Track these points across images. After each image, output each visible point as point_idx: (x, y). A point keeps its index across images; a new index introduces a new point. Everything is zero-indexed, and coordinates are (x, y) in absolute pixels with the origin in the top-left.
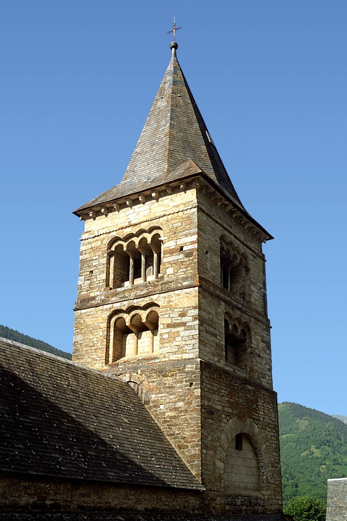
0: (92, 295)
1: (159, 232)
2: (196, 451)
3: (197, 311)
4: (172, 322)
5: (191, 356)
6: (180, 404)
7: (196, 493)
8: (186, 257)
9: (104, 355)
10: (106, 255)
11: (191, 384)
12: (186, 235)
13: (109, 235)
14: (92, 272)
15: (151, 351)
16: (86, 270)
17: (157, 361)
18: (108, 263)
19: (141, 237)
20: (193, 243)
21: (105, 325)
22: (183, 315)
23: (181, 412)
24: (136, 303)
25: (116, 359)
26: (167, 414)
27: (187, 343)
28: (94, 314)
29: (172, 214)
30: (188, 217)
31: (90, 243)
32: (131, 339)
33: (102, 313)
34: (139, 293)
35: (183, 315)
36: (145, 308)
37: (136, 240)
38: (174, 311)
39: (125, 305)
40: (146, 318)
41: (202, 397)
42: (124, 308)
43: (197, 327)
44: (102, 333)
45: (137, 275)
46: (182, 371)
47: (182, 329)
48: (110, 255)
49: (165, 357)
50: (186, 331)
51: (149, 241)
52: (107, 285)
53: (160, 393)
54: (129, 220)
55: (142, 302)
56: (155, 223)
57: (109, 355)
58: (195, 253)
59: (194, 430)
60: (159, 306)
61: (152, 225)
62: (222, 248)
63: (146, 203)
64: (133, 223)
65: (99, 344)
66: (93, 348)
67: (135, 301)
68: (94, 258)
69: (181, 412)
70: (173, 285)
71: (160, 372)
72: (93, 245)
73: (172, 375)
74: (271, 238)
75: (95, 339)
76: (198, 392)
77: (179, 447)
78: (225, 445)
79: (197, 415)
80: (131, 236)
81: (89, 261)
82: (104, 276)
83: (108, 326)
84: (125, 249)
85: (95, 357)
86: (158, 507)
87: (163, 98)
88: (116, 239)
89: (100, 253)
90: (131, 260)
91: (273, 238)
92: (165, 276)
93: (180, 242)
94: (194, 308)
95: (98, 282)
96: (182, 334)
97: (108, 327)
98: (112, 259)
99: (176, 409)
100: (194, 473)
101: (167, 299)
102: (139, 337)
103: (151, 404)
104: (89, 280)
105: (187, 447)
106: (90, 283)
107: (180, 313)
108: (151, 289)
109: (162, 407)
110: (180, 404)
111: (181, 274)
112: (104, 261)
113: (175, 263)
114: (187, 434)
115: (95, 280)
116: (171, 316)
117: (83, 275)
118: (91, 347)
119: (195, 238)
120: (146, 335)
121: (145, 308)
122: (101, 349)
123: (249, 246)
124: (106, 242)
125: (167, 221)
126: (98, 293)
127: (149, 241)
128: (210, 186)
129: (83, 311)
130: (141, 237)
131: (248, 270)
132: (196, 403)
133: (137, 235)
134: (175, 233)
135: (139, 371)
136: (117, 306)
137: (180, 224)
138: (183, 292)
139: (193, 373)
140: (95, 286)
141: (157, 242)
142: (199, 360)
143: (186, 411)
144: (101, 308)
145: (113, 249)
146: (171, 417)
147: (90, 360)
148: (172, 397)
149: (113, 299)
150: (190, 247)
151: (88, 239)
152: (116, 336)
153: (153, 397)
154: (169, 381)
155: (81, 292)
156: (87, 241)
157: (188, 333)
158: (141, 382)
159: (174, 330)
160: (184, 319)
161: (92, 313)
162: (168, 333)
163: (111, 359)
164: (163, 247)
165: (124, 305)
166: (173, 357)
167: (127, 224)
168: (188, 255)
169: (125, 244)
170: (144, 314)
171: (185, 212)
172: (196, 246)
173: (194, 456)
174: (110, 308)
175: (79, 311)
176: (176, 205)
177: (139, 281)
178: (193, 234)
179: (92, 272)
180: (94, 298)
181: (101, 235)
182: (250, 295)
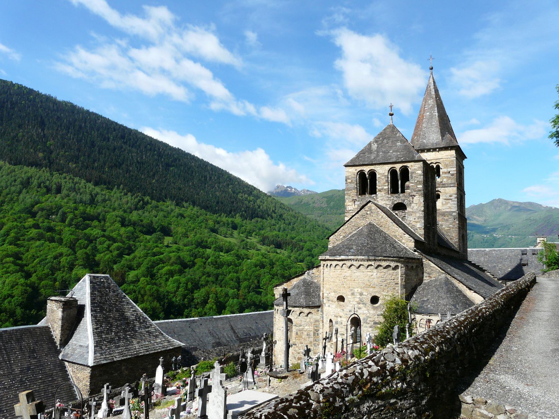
1: (439, 164)
3: (456, 196)
5: (454, 210)
12: (451, 168)
20: (454, 171)
22: (451, 196)
35: (451, 196)
46: (451, 215)
47: (450, 201)
51: (435, 167)
56: (438, 161)
58: (455, 175)
70: (446, 185)
76: (457, 222)
77: (451, 239)
93: (449, 170)
96: (450, 203)
99: (449, 227)
100: (456, 247)
111: (450, 181)
113: (447, 177)
119: (455, 169)
127: (435, 167)
132: (457, 226)
134: (446, 166)
150: (453, 172)
153: (440, 223)
154: (446, 218)
157: (453, 202)
159: (447, 201)
160: (451, 198)
166: (448, 210)
168: (452, 175)
172: (456, 172)
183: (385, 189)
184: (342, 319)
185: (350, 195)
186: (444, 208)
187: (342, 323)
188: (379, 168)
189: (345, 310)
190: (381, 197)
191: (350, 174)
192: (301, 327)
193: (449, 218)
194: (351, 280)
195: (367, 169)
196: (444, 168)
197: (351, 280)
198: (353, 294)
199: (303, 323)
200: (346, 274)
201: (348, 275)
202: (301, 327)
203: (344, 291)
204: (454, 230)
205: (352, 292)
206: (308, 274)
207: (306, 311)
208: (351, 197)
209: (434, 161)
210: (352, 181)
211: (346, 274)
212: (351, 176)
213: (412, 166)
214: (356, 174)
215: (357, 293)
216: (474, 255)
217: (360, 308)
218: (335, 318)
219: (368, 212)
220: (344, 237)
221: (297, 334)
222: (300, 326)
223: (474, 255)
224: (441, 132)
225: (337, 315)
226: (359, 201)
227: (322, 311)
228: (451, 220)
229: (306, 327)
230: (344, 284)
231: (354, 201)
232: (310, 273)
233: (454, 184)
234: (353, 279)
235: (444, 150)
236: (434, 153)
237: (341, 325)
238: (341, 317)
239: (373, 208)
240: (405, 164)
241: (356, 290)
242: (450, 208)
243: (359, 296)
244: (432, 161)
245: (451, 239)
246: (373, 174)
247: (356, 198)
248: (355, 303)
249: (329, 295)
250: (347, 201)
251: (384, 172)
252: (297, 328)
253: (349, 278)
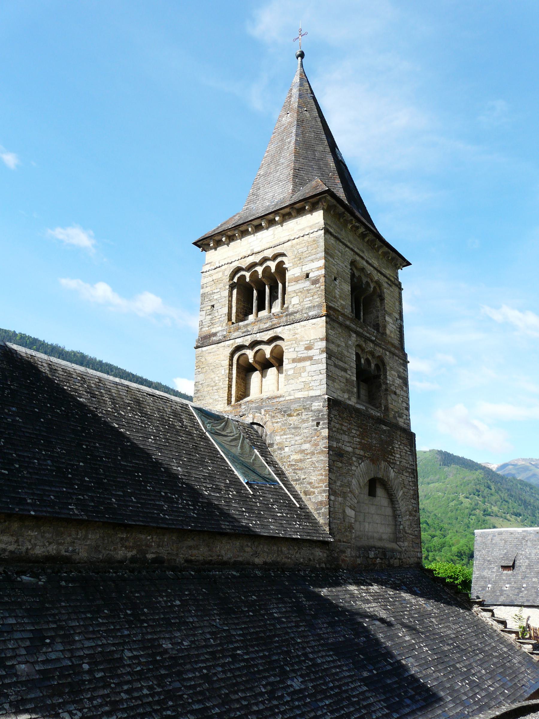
0: (214, 331)
2: (323, 497)
3: (323, 344)
4: (297, 356)
5: (318, 393)
6: (306, 446)
7: (325, 543)
8: (312, 284)
9: (226, 395)
10: (228, 287)
11: (318, 424)
12: (312, 261)
13: (231, 265)
14: (213, 306)
15: (275, 389)
16: (208, 304)
17: (281, 399)
18: (231, 295)
19: (264, 266)
20: (319, 269)
21: (227, 362)
22: (309, 348)
23: (307, 454)
25: (239, 399)
26: (292, 457)
27: (314, 378)
28: (216, 351)
29: (297, 238)
30: (314, 241)
31: (211, 275)
32: (256, 377)
33: (225, 349)
34: (263, 326)
35: (309, 348)
36: (270, 342)
37: (260, 270)
38: (299, 344)
39: (247, 341)
40: (270, 353)
41: (330, 438)
42: (247, 344)
43: (324, 361)
44: (224, 371)
45: (261, 307)
47: (308, 363)
48: (232, 287)
49: (290, 395)
50: (312, 366)
51: (273, 270)
52: (230, 319)
53: (284, 434)
54: (251, 248)
55: (266, 336)
56: (278, 250)
57: (231, 395)
58: (322, 280)
59: (322, 475)
60: (283, 339)
61: (276, 252)
62: (353, 275)
63: (269, 229)
64: (256, 250)
65: (221, 383)
66: (215, 388)
68: (216, 291)
69: (307, 454)
70: (298, 316)
71: (285, 412)
72: (215, 277)
73: (298, 414)
74: (411, 264)
75: (217, 378)
76: (325, 432)
77: (306, 493)
78: (356, 490)
79: (324, 458)
80: (254, 265)
81: (211, 294)
82: (226, 310)
83: (230, 364)
84: (248, 280)
85: (217, 397)
86: (278, 560)
87: (288, 113)
88: (239, 269)
89: (222, 285)
90: (255, 292)
91: (411, 264)
92: (290, 307)
93: (306, 269)
94: (322, 340)
95: (220, 316)
96: (308, 369)
97: (231, 365)
98: (235, 292)
99: (302, 451)
101: (292, 332)
102: (263, 375)
103: (275, 447)
104: (210, 314)
105: (314, 493)
106: (211, 318)
107: (306, 346)
108: (275, 321)
109: (287, 449)
110: (306, 446)
111: (307, 303)
112: (226, 293)
114: (314, 478)
116: (296, 350)
117: (204, 309)
119: (322, 262)
120: (272, 372)
121: (270, 342)
122: (222, 388)
123: (384, 272)
124: (228, 273)
125: (292, 246)
126: (220, 328)
127: (273, 270)
128: (338, 205)
129: (204, 349)
130: (264, 266)
131: (382, 299)
132: (323, 444)
133: (261, 263)
134: (300, 259)
135: (263, 411)
136: (239, 342)
137: (305, 249)
138: (310, 323)
139: (320, 411)
141: (281, 270)
142: (326, 397)
143: (313, 454)
144: (222, 344)
145: (235, 280)
146: (297, 461)
147: (211, 401)
148: (297, 438)
151: (209, 271)
152: (239, 375)
153: (278, 439)
154: (293, 420)
156: (208, 273)
157: (314, 368)
158: (265, 423)
159: (300, 365)
160: (310, 353)
161: (213, 350)
162: (294, 368)
163: (233, 399)
164: (288, 275)
166: (299, 395)
167: (249, 253)
168: (315, 282)
169: (248, 275)
170: (267, 350)
171: (311, 235)
172: (323, 272)
173: (321, 503)
174: (232, 344)
175: (200, 349)
176: (301, 228)
177: (263, 314)
178: (320, 259)
179: (213, 306)
180: (215, 334)
181: (222, 265)
182: (385, 327)
186: (290, 388)
193: (304, 421)
196: (295, 265)
204: (314, 459)
209: (269, 254)
216: (529, 544)
223: (529, 544)
224: (295, 176)
228: (307, 428)
233: (319, 306)
235: (295, 217)
242: (307, 386)
245: (306, 493)
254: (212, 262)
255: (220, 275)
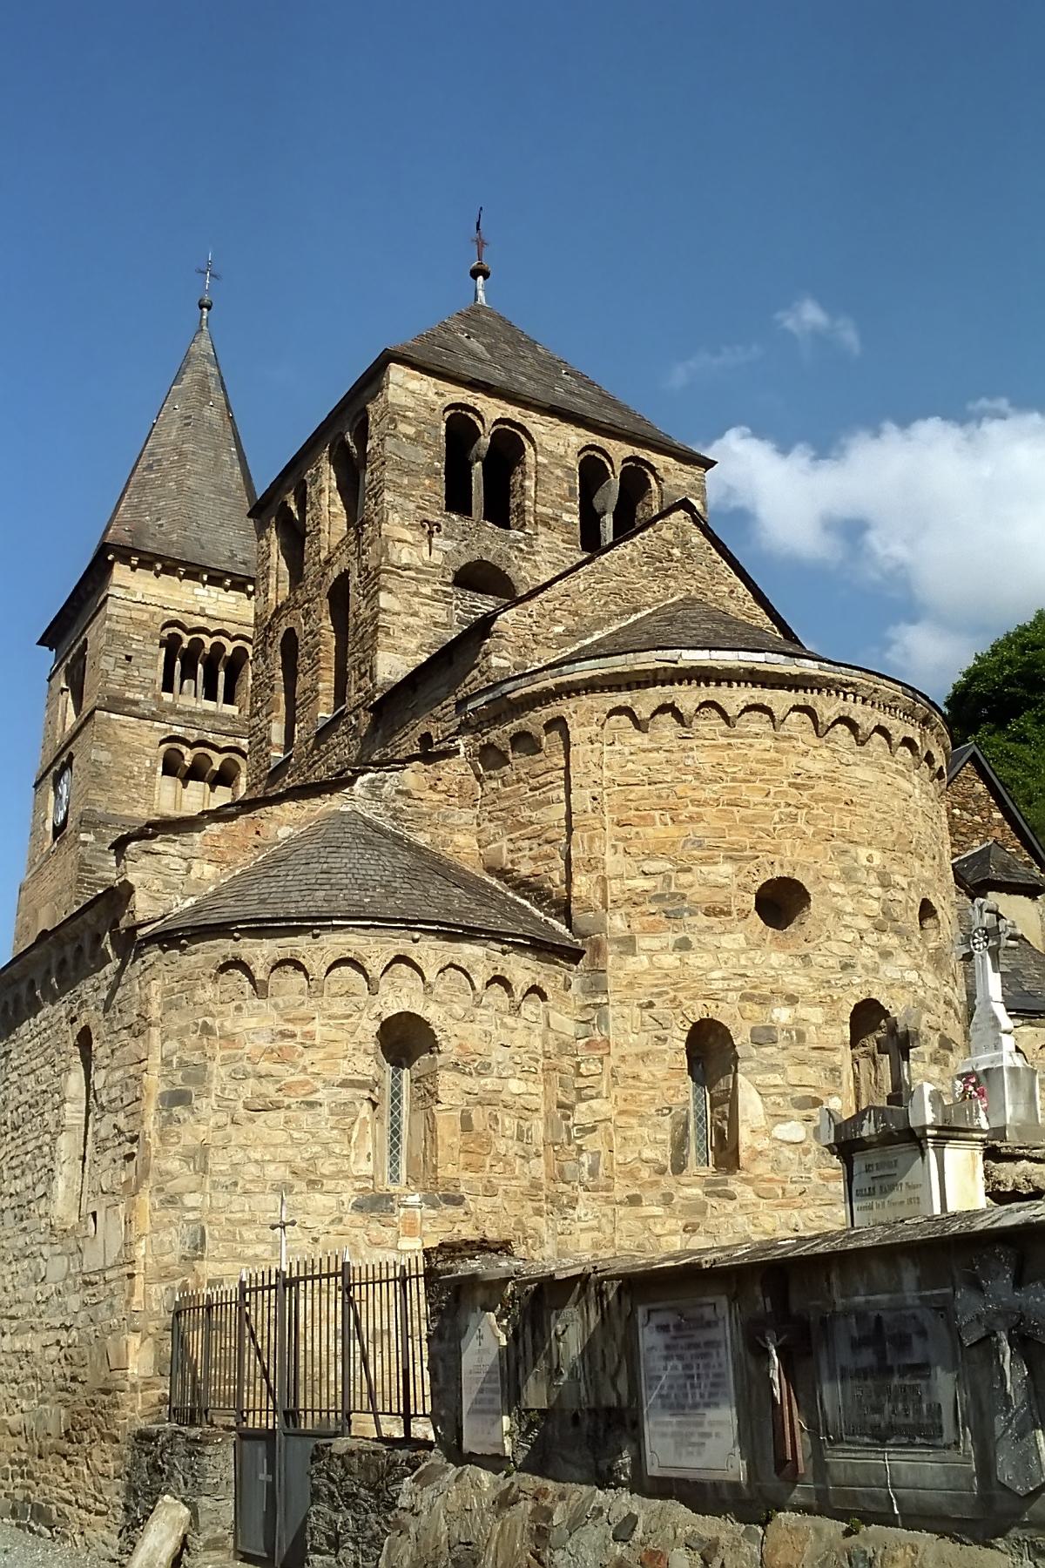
0: (128, 695)
13: (165, 612)
14: (129, 658)
24: (210, 737)
28: (133, 728)
34: (218, 725)
39: (194, 735)
63: (230, 592)
64: (208, 612)
65: (143, 779)
67: (211, 735)
68: (136, 637)
72: (134, 614)
75: (136, 769)
84: (185, 645)
85: (136, 796)
104: (123, 668)
115: (136, 674)
118: (128, 778)
126: (141, 697)
127: (229, 652)
129: (113, 716)
136: (178, 730)
140: (137, 683)
144: (149, 723)
145: (165, 634)
147: (124, 798)
149: (173, 718)
155: (106, 682)
156: (119, 601)
161: (132, 725)
165: (192, 735)
169: (187, 639)
170: (217, 760)
174: (166, 731)
175: (105, 713)
180: (136, 703)
183: (567, 525)
184: (803, 1011)
185: (407, 496)
187: (801, 1037)
188: (541, 428)
189: (817, 959)
190: (550, 550)
191: (410, 402)
192: (490, 1083)
194: (836, 800)
195: (492, 410)
197: (836, 800)
198: (848, 876)
199: (498, 1055)
200: (806, 763)
201: (817, 767)
202: (490, 1083)
203: (802, 856)
205: (847, 861)
206: (373, 787)
207: (522, 969)
208: (412, 506)
210: (419, 433)
211: (806, 763)
212: (413, 410)
213: (667, 470)
214: (439, 410)
215: (868, 869)
217: (886, 954)
218: (752, 1009)
219: (676, 552)
220: (570, 633)
221: (466, 1123)
222: (484, 1069)
225: (765, 990)
226: (449, 537)
227: (596, 985)
229: (515, 1086)
230: (794, 818)
231: (430, 529)
232: (387, 788)
234: (846, 797)
236: (233, 595)
237: (797, 1049)
238: (792, 1000)
239: (695, 540)
240: (644, 454)
241: (863, 853)
243: (877, 891)
244: (227, 626)
246: (509, 447)
247: (436, 519)
248: (864, 924)
249: (685, 878)
250: (395, 517)
251: (561, 450)
252: (468, 1083)
253: (823, 788)
254: (128, 588)
255: (146, 617)
